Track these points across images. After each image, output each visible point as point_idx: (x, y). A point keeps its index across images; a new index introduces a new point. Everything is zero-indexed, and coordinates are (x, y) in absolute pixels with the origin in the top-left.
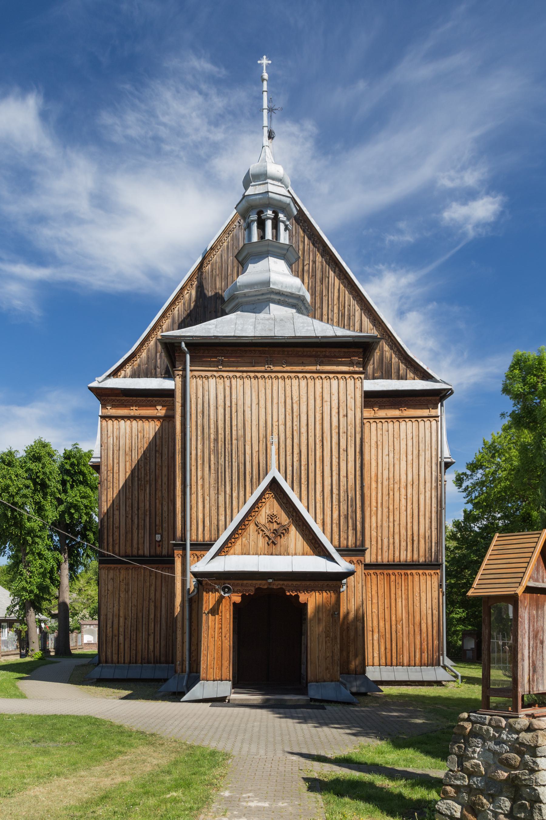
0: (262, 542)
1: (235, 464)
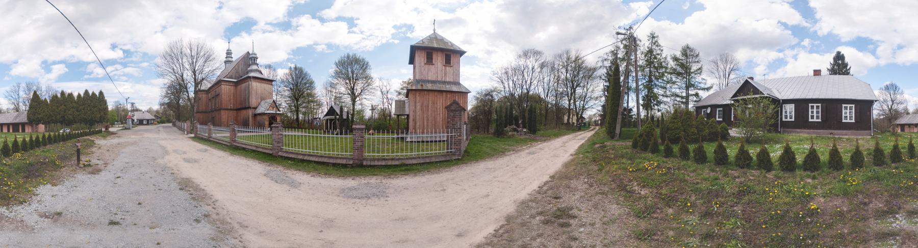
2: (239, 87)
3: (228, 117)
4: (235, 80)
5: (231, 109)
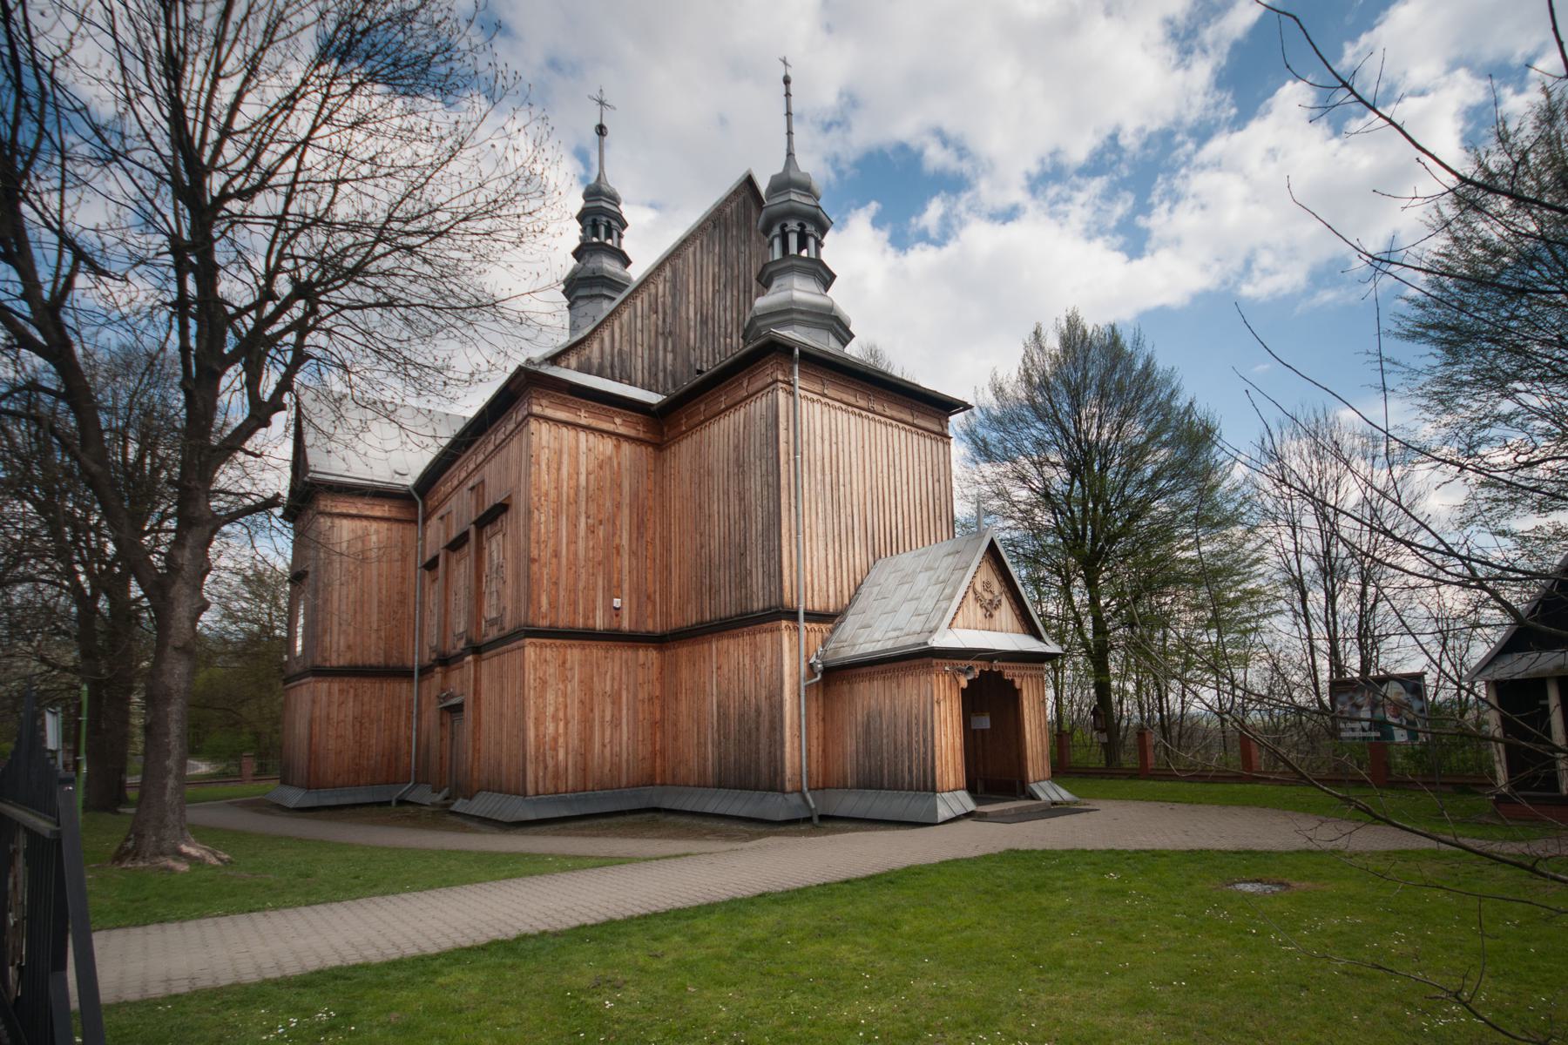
0: (980, 612)
1: (843, 516)
2: (684, 452)
3: (587, 706)
4: (653, 398)
5: (613, 637)
